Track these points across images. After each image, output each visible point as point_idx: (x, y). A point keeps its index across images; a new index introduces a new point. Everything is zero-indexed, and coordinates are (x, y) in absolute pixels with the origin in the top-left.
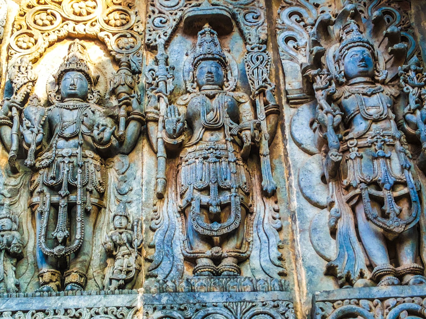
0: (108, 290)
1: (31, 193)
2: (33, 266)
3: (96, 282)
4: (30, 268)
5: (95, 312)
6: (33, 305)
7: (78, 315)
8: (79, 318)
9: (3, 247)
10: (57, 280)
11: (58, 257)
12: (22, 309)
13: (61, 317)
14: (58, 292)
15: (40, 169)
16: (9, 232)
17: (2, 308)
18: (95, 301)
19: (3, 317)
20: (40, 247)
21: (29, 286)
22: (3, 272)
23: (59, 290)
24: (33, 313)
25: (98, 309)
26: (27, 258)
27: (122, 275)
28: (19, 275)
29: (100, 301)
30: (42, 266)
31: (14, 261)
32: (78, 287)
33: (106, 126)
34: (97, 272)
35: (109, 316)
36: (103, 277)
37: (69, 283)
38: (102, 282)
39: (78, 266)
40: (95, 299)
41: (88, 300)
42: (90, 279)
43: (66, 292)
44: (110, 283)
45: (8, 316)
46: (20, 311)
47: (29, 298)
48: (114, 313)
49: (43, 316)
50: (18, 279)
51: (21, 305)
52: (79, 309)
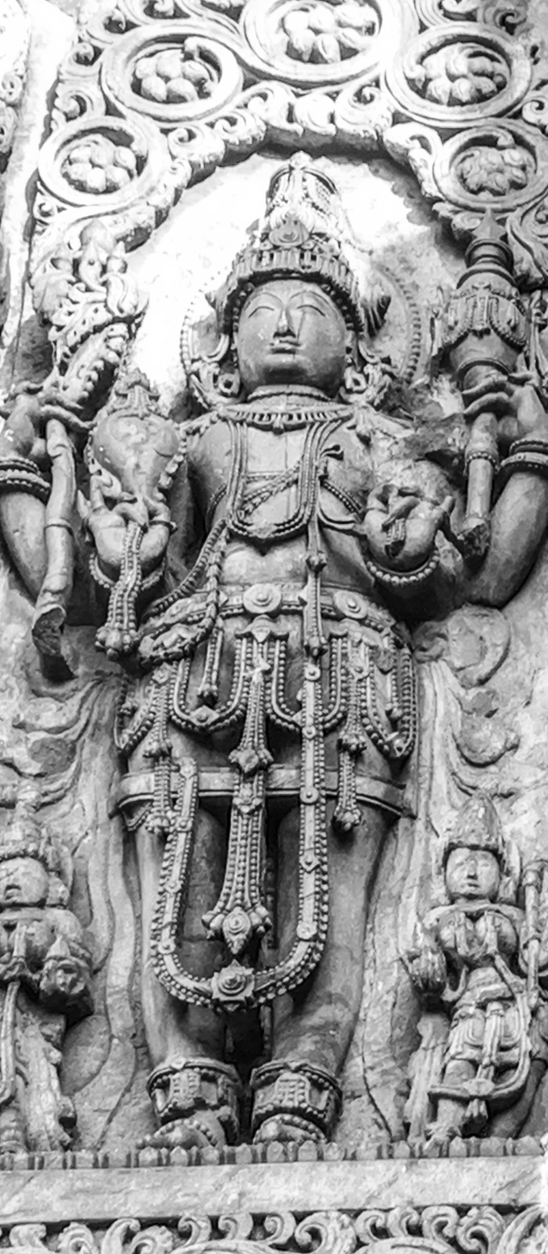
0: (422, 1138)
1: (123, 760)
2: (129, 1045)
3: (377, 1110)
4: (117, 1051)
5: (373, 1227)
6: (131, 1198)
7: (304, 1237)
8: (308, 1248)
9: (11, 969)
10: (222, 1102)
11: (226, 1012)
12: (85, 1217)
13: (241, 1248)
14: (226, 1149)
15: (155, 663)
16: (37, 913)
17: (7, 1210)
18: (371, 1185)
19: (10, 1245)
20: (157, 970)
21: (113, 1124)
22: (11, 1071)
23: (232, 1141)
24: (128, 1229)
25: (382, 1215)
26: (106, 1014)
27: (477, 1079)
28: (72, 1081)
29: (390, 1184)
30: (166, 1048)
31: (56, 1027)
32: (306, 1128)
33: (417, 494)
34: (379, 1069)
35: (427, 1242)
36: (405, 1089)
37: (269, 1114)
38: (401, 1109)
39: (307, 1045)
40: (373, 1174)
41: (346, 1179)
42: (354, 1096)
43: (259, 1148)
44: (434, 1115)
45: (33, 1244)
46: (80, 1221)
47: (114, 1172)
48: (447, 1231)
49: (169, 1244)
50: (70, 1095)
51: (82, 1197)
52: (310, 1213)
